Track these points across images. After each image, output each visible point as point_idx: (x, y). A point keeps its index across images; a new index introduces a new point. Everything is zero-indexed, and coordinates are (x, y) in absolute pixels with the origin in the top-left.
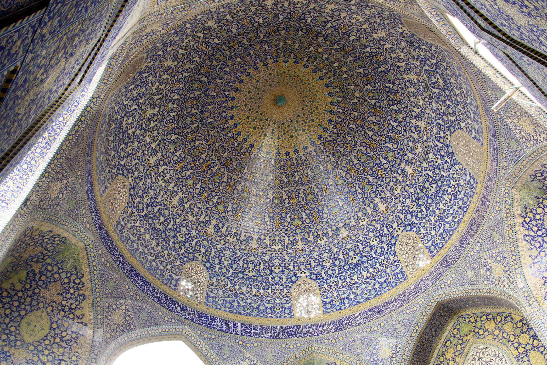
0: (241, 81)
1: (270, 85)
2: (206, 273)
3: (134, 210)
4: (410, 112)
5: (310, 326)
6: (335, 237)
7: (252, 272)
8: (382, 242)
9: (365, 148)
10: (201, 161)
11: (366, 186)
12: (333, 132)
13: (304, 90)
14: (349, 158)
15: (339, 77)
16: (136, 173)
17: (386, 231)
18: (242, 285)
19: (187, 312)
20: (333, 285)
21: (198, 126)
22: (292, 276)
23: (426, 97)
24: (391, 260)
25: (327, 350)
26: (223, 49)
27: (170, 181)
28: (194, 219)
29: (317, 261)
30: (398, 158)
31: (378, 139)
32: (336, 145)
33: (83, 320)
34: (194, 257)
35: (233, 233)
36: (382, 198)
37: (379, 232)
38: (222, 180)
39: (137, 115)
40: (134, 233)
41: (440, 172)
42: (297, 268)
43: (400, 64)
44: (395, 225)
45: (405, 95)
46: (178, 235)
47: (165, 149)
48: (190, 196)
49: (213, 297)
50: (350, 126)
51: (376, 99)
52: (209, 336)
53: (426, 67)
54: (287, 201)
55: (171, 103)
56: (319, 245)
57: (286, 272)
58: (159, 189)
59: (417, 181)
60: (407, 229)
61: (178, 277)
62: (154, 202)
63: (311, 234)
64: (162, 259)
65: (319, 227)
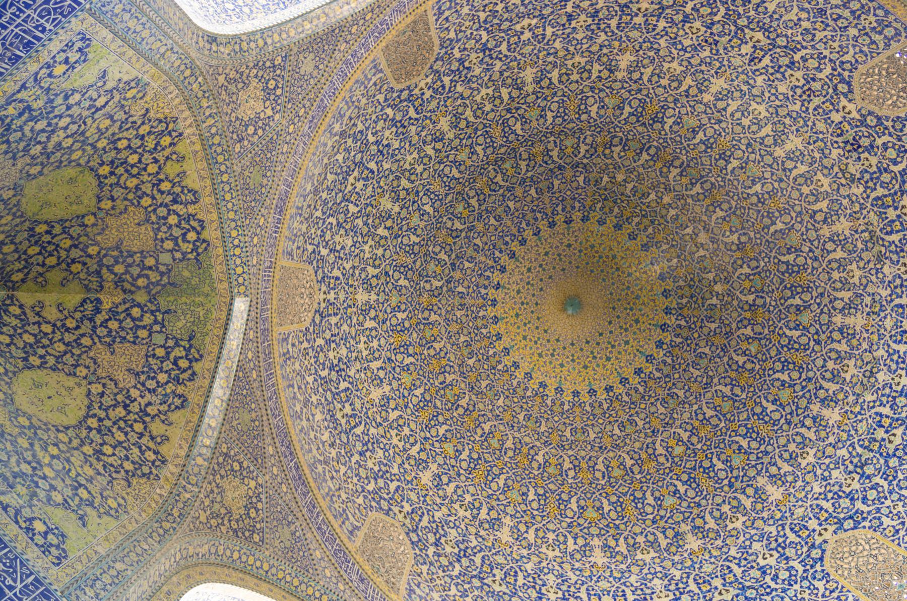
0: (523, 242)
1: (563, 270)
4: (831, 302)
9: (729, 387)
10: (432, 352)
14: (695, 407)
16: (332, 292)
17: (792, 537)
23: (869, 262)
28: (401, 445)
30: (803, 396)
31: (758, 367)
32: (670, 385)
33: (160, 449)
34: (390, 509)
35: (466, 502)
36: (771, 476)
37: (776, 540)
38: (459, 402)
39: (370, 189)
43: (816, 207)
44: (813, 524)
45: (820, 270)
53: (880, 192)
54: (571, 473)
55: (417, 215)
56: (641, 563)
59: (853, 432)
63: (622, 540)
65: (637, 530)
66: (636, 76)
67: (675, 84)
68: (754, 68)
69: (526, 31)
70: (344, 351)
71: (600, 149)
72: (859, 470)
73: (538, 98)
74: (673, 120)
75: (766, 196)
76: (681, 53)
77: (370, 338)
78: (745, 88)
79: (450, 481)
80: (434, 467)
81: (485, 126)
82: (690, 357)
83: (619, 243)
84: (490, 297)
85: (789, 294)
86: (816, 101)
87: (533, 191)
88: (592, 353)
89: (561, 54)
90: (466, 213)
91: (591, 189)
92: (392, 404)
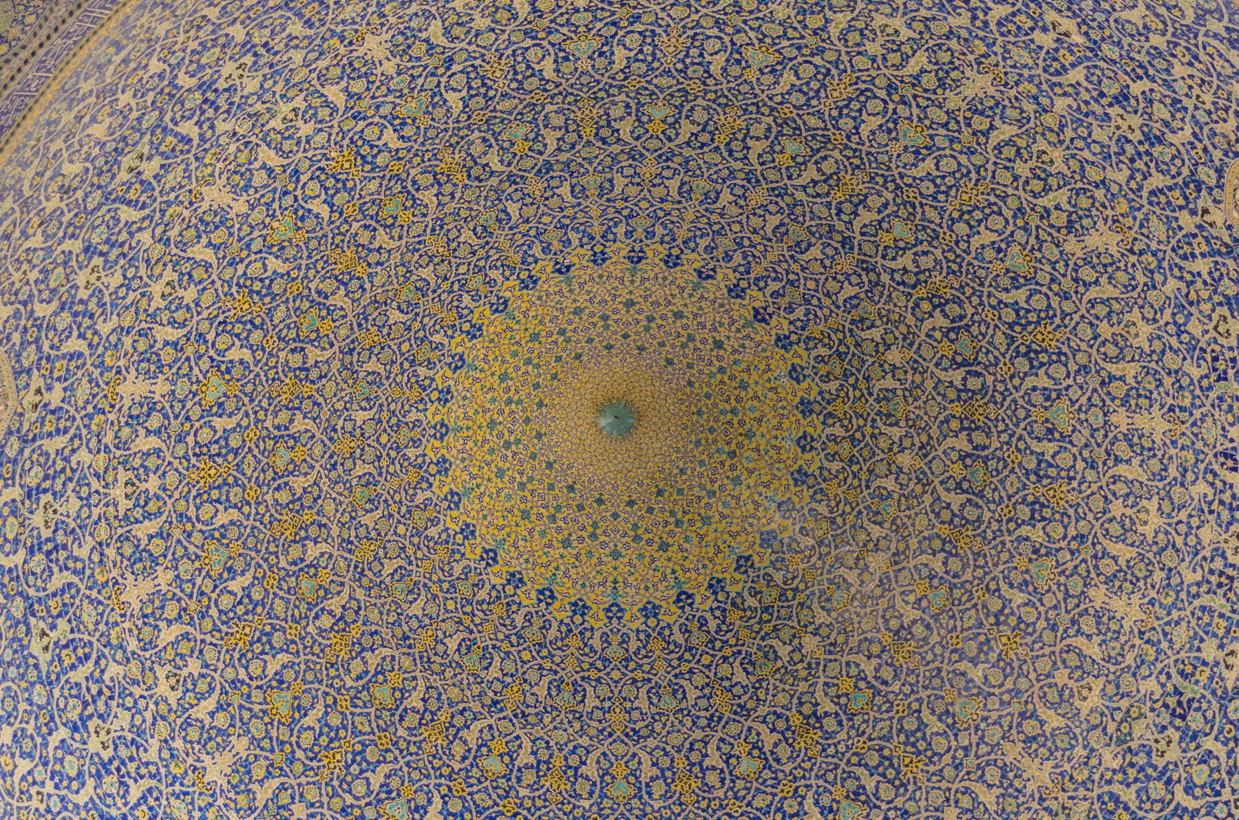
1: (670, 362)
7: (46, 648)
10: (364, 237)
12: (624, 641)
13: (701, 475)
14: (584, 741)
31: (721, 794)
32: (594, 674)
34: (29, 371)
35: (143, 486)
45: (944, 785)
48: (236, 246)
50: (685, 683)
54: (326, 621)
55: (596, 44)
63: (275, 783)
66: (1087, 274)
67: (1111, 350)
68: (1216, 467)
69: (1052, 35)
70: (252, 86)
71: (922, 292)
73: (945, 126)
74: (1048, 383)
75: (1013, 621)
76: (1172, 329)
77: (309, 114)
78: (1173, 472)
79: (157, 432)
80: (161, 387)
82: (662, 675)
83: (779, 427)
84: (535, 269)
85: (872, 763)
86: (1218, 603)
88: (558, 508)
89: (1049, 120)
90: (656, 128)
91: (843, 319)
92: (219, 236)
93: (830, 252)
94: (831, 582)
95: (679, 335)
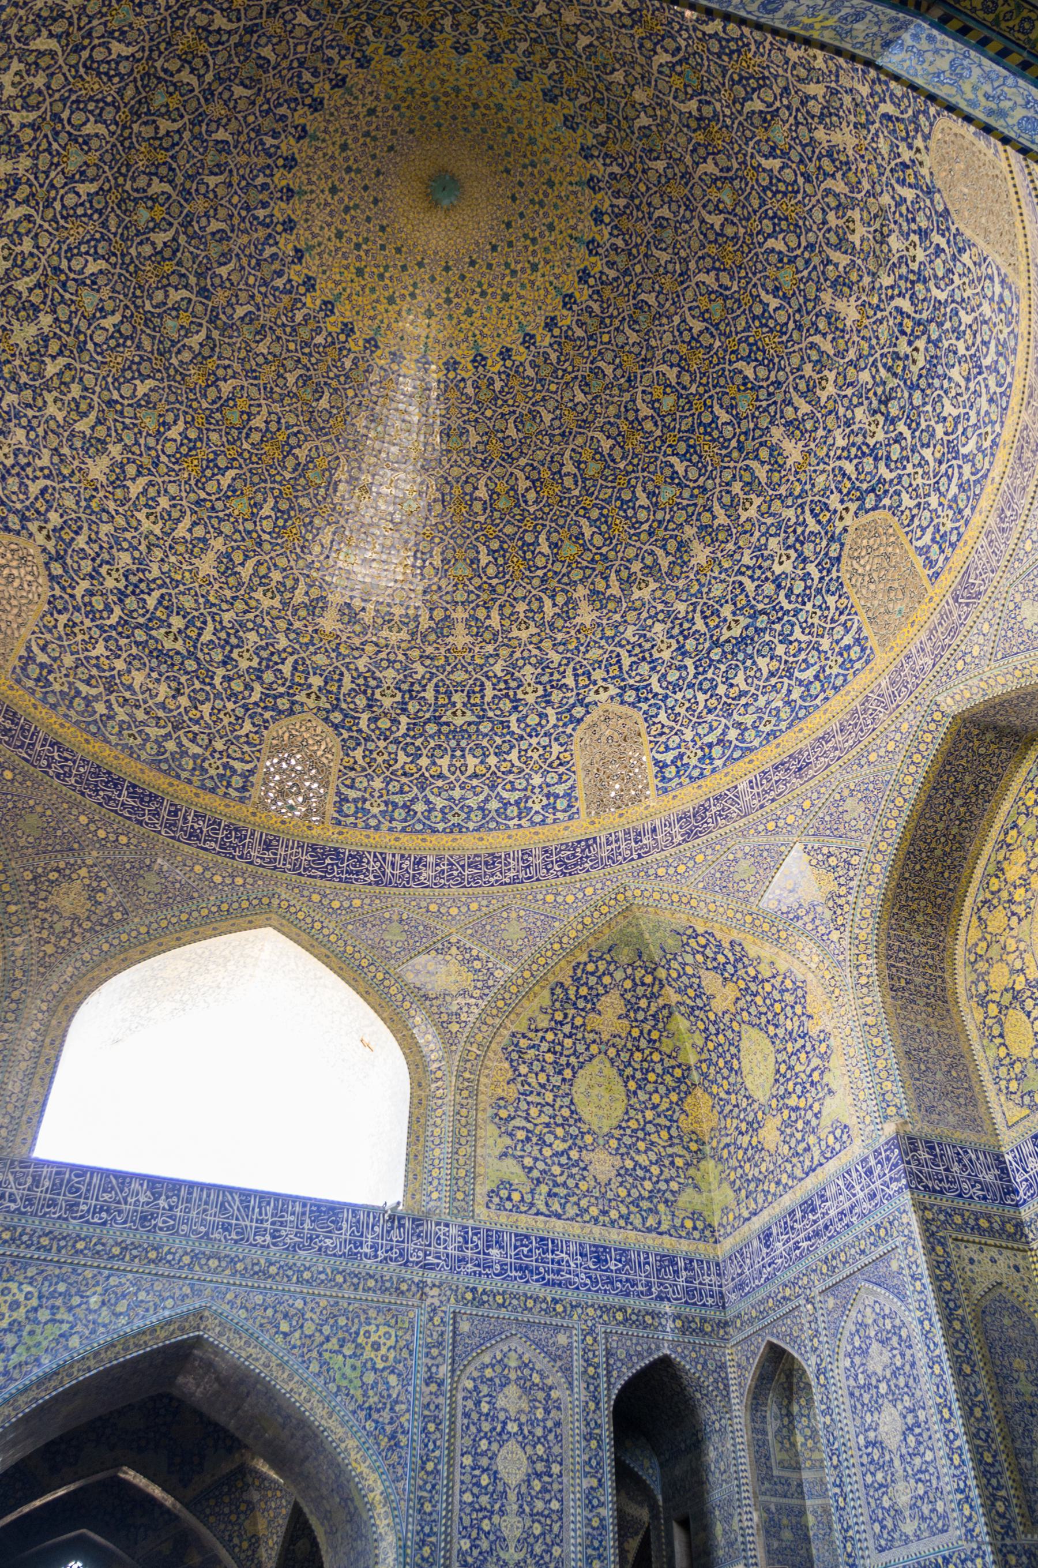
0: (290, 163)
1: (391, 149)
2: (332, 740)
3: (77, 618)
4: (802, 103)
5: (621, 835)
6: (677, 570)
8: (804, 561)
10: (256, 437)
11: (738, 396)
14: (677, 319)
15: (570, 54)
17: (812, 526)
18: (438, 753)
19: (281, 852)
20: (683, 711)
21: (208, 337)
22: (574, 706)
24: (832, 610)
25: (665, 896)
26: (165, 71)
27: (175, 514)
29: (637, 650)
30: (809, 279)
31: (742, 231)
32: (633, 287)
34: (293, 703)
35: (396, 618)
36: (788, 423)
40: (92, 677)
41: (928, 290)
42: (583, 681)
44: (834, 502)
46: (235, 655)
47: (125, 427)
48: (249, 543)
49: (355, 801)
51: (696, 93)
52: (346, 904)
54: (532, 496)
55: (85, 291)
56: (638, 604)
57: (556, 696)
58: (144, 543)
59: (874, 341)
60: (868, 506)
61: (248, 767)
62: (141, 581)
64: (196, 728)
70: (125, 559)
72: (883, 408)
77: (151, 504)
81: (63, 100)
83: (449, 67)
87: (239, 91)
88: (507, 265)
92: (238, 557)
93: (263, 40)
94: (589, 59)
95: (365, 144)
